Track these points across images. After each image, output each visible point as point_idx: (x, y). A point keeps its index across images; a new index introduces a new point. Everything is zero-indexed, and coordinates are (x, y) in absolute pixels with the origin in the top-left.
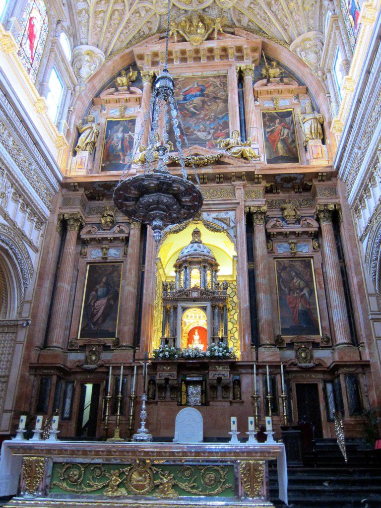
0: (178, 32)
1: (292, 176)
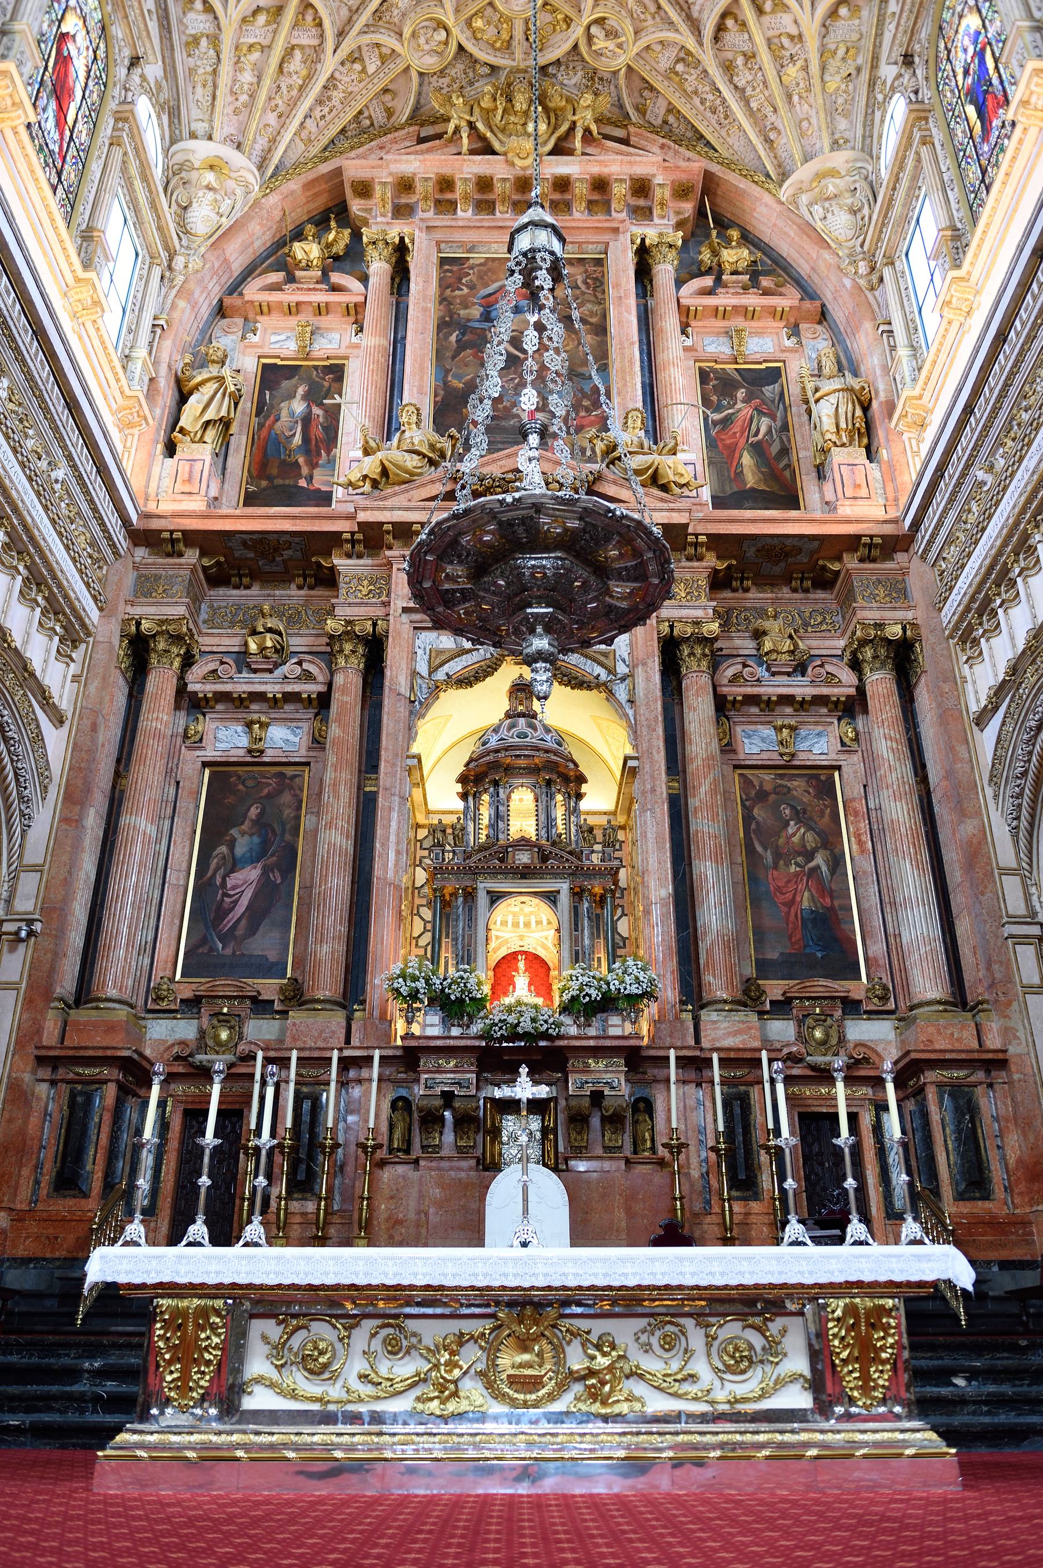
0: (471, 125)
1: (788, 542)
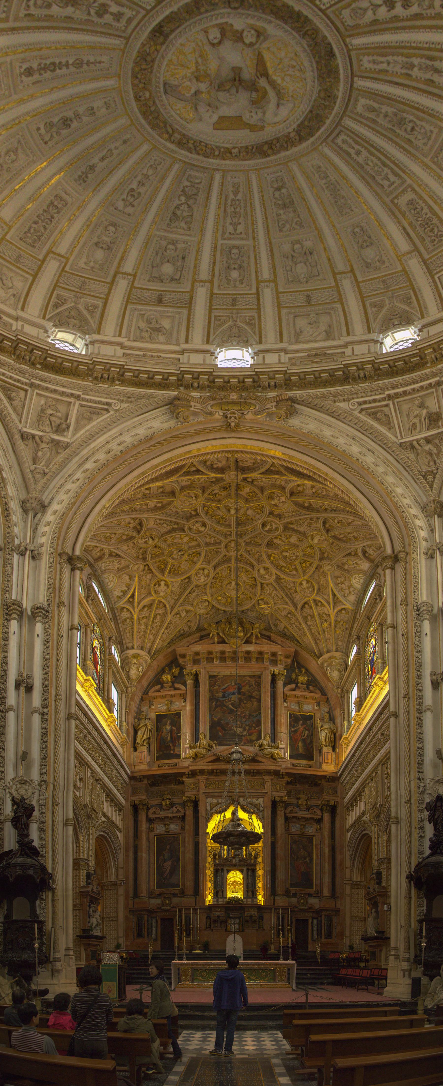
0: (218, 634)
